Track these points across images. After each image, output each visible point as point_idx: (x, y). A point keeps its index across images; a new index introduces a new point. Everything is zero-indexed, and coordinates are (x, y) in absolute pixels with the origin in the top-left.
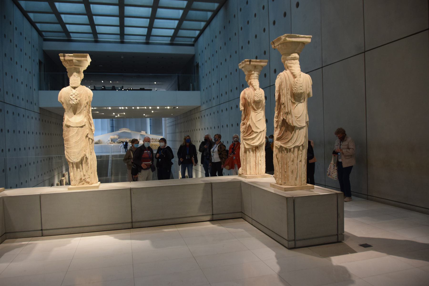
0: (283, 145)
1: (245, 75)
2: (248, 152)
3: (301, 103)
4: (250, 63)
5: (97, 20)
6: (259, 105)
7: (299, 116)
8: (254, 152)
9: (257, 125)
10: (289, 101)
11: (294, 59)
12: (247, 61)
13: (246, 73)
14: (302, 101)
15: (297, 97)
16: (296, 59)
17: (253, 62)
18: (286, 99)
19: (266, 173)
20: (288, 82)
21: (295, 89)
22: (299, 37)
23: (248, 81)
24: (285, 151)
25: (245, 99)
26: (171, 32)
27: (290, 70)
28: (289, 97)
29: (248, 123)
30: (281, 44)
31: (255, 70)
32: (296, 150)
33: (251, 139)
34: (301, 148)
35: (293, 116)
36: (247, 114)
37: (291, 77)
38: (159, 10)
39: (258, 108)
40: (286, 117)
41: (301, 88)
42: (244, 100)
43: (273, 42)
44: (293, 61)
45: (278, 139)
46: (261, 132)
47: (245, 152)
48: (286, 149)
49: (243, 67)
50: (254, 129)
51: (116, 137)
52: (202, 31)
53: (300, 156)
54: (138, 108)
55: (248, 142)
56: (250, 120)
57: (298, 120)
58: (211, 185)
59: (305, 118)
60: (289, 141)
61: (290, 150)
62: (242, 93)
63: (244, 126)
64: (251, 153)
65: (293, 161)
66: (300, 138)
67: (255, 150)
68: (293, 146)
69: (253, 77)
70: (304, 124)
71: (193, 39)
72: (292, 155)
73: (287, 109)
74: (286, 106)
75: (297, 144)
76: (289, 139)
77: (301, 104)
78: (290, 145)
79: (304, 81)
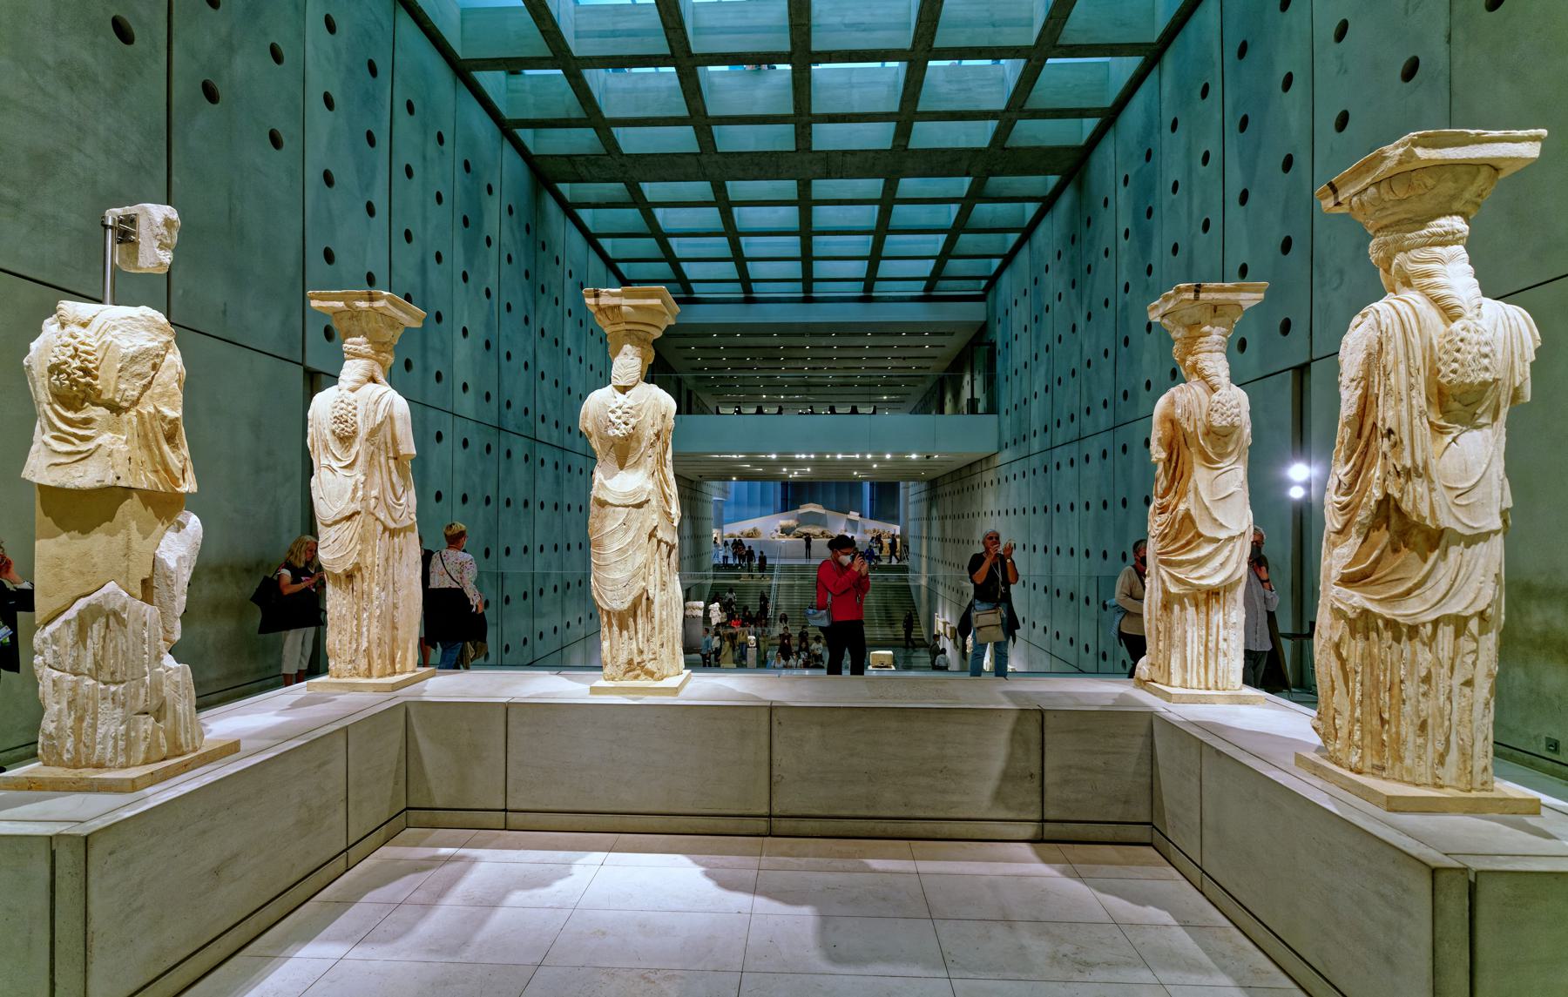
0: (1375, 608)
1: (1172, 342)
2: (1176, 608)
4: (1197, 298)
5: (750, 246)
6: (1226, 444)
7: (1468, 484)
8: (1203, 609)
9: (1216, 515)
10: (1416, 422)
11: (1444, 240)
12: (1187, 290)
13: (1178, 333)
14: (1482, 420)
15: (1456, 403)
16: (1456, 242)
17: (1209, 290)
18: (1404, 414)
19: (1246, 681)
20: (1416, 341)
22: (1479, 140)
23: (1184, 361)
24: (1388, 635)
25: (1173, 422)
26: (926, 268)
27: (1423, 290)
28: (1420, 401)
29: (1182, 507)
30: (1377, 184)
31: (1215, 321)
32: (1447, 632)
33: (1191, 562)
34: (1474, 625)
35: (1438, 486)
36: (1177, 472)
37: (1432, 315)
38: (897, 209)
39: (1222, 456)
40: (1402, 490)
41: (1486, 361)
42: (1168, 425)
43: (1331, 186)
44: (1438, 249)
45: (1348, 581)
46: (1231, 539)
47: (1167, 606)
48: (1391, 624)
49: (1163, 316)
50: (1206, 529)
51: (792, 523)
52: (1008, 259)
53: (1469, 659)
54: (839, 456)
55: (1179, 573)
56: (1191, 495)
57: (1458, 501)
58: (1039, 717)
59: (1497, 494)
60: (1408, 593)
61: (1413, 631)
62: (1162, 401)
63: (1164, 517)
64: (1191, 611)
65: (1427, 679)
66: (1473, 580)
67: (1207, 603)
68: (1433, 616)
69: (1205, 347)
70: (1497, 524)
71: (984, 283)
72: (1425, 656)
73: (1407, 453)
74: (1406, 442)
75: (1454, 607)
76: (1410, 584)
78: (1411, 610)
79: (1501, 333)
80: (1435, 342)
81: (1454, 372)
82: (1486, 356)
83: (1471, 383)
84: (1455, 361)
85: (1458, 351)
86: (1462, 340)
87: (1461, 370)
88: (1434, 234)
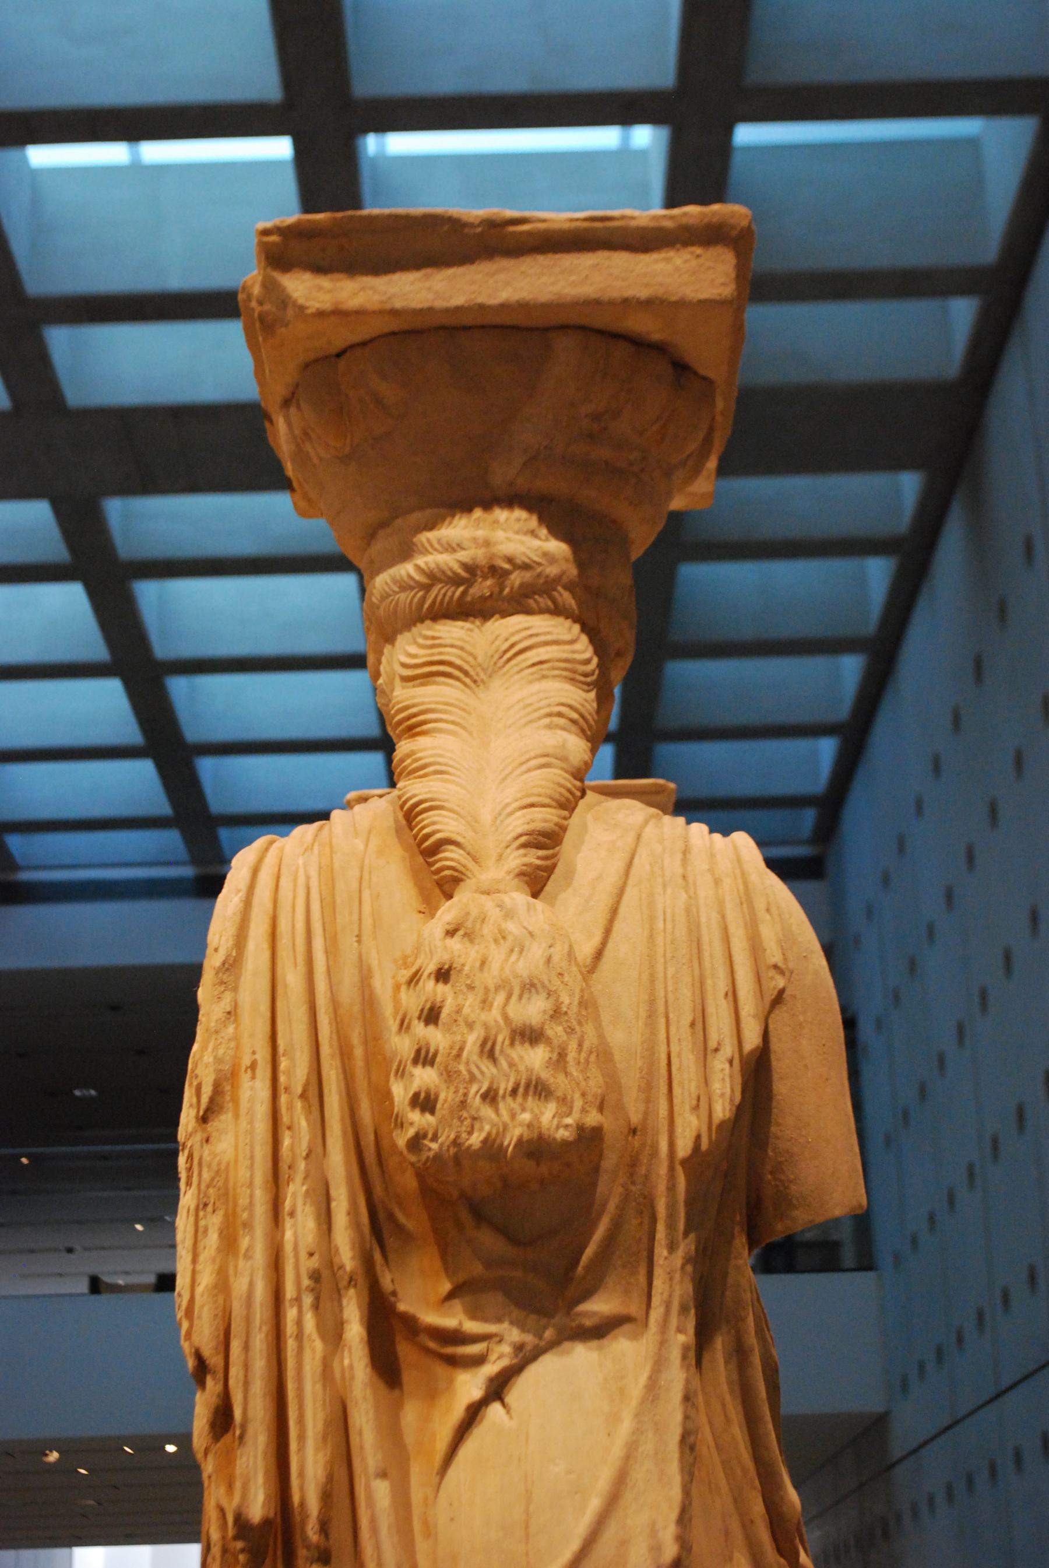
3: (600, 1331)
10: (302, 1318)
11: (479, 595)
21: (424, 1077)
37: (393, 878)
41: (535, 1059)
44: (452, 631)
73: (253, 1458)
74: (253, 1408)
77: (582, 1357)
80: (382, 986)
81: (425, 1102)
82: (531, 1036)
83: (491, 1149)
84: (424, 1057)
85: (432, 1016)
86: (443, 975)
87: (446, 1097)
88: (434, 577)
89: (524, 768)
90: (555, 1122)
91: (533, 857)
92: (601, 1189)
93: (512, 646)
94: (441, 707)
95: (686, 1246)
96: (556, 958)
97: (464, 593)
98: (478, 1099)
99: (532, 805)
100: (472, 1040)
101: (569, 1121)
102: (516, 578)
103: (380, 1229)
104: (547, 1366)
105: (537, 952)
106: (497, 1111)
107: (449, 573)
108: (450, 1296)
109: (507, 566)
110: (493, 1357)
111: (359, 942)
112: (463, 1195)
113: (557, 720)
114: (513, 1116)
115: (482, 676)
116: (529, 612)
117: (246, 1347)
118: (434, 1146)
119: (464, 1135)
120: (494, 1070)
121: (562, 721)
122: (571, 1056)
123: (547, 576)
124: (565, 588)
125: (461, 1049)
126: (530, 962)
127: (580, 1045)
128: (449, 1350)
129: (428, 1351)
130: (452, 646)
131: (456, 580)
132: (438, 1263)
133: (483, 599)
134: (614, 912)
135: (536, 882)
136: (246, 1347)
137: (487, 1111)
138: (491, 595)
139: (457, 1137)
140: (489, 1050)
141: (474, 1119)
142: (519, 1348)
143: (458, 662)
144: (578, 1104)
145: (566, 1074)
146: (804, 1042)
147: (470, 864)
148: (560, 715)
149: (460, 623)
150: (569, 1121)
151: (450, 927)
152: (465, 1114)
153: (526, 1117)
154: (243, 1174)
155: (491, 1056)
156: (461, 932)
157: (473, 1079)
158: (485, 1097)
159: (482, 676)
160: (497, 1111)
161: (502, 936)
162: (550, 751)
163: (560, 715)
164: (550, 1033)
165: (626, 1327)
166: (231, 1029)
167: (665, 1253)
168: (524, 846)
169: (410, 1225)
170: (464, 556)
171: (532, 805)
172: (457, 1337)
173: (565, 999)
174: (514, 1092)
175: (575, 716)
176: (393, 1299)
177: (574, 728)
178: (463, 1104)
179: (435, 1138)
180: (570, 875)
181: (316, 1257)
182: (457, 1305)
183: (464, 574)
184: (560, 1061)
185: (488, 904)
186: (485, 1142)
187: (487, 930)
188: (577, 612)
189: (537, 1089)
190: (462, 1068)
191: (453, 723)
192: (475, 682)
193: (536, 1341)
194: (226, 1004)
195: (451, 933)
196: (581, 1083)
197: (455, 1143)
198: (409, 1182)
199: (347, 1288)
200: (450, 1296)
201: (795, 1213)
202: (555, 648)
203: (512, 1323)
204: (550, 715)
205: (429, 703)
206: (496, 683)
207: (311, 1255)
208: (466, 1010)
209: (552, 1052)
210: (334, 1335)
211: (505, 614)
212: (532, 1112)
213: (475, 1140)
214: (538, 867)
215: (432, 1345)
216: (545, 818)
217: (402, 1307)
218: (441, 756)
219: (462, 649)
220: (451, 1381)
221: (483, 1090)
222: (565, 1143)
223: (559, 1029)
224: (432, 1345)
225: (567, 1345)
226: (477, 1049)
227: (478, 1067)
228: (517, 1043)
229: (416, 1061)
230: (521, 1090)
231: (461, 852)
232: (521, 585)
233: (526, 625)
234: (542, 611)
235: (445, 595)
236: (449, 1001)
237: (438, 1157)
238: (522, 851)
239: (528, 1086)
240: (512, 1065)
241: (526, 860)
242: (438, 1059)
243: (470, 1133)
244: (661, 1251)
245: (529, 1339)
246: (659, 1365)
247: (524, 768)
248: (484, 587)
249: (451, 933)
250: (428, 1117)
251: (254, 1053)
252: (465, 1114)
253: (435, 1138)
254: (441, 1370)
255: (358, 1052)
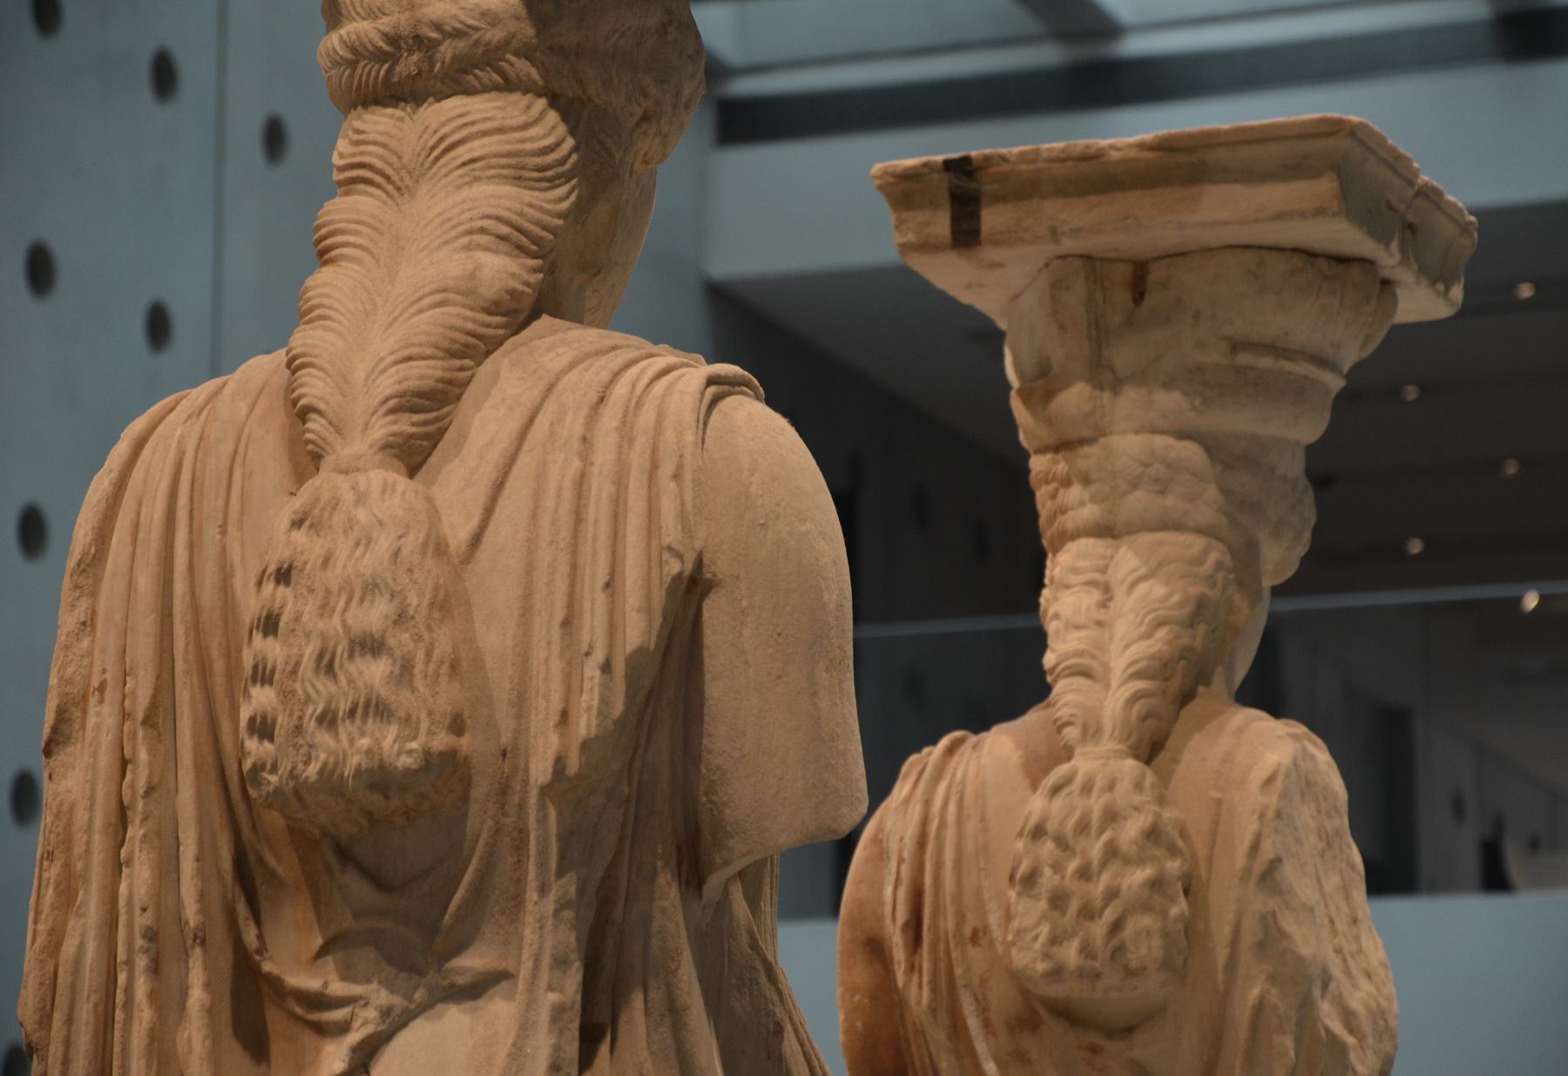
3: (474, 990)
14: (472, 961)
21: (262, 698)
37: (268, 451)
41: (376, 671)
77: (454, 1018)
81: (263, 728)
82: (370, 645)
83: (330, 780)
84: (262, 675)
86: (284, 575)
87: (283, 723)
89: (416, 307)
90: (396, 748)
91: (406, 424)
92: (472, 822)
93: (441, 140)
94: (351, 226)
95: (568, 885)
96: (405, 552)
97: (389, 72)
98: (313, 723)
99: (410, 359)
100: (310, 651)
101: (414, 745)
102: (447, 50)
103: (248, 879)
104: (417, 1033)
105: (384, 545)
106: (336, 736)
107: (370, 47)
108: (323, 952)
109: (434, 35)
110: (356, 1024)
111: (224, 533)
112: (325, 833)
113: (478, 238)
114: (351, 741)
115: (408, 181)
116: (468, 91)
117: (69, 1020)
118: (274, 779)
119: (300, 766)
120: (333, 688)
121: (484, 239)
122: (419, 667)
123: (488, 44)
124: (517, 54)
125: (298, 664)
126: (373, 560)
127: (429, 655)
128: (315, 1016)
129: (298, 1018)
130: (375, 143)
131: (379, 56)
132: (311, 914)
133: (413, 78)
134: (499, 486)
135: (413, 455)
136: (69, 1020)
137: (324, 738)
138: (419, 73)
139: (293, 768)
140: (327, 665)
141: (311, 746)
142: (386, 1012)
143: (379, 164)
144: (424, 725)
145: (413, 690)
146: (747, 633)
147: (331, 436)
148: (482, 231)
149: (390, 111)
150: (414, 745)
151: (296, 517)
152: (301, 741)
153: (365, 742)
154: (81, 817)
155: (330, 670)
156: (307, 523)
157: (308, 700)
158: (320, 720)
159: (408, 181)
160: (336, 736)
161: (351, 523)
162: (451, 283)
163: (482, 231)
164: (392, 642)
165: (504, 984)
166: (85, 643)
167: (535, 897)
168: (392, 411)
169: (280, 870)
170: (385, 23)
171: (410, 359)
172: (319, 1001)
173: (413, 600)
174: (352, 713)
175: (505, 230)
176: (257, 958)
177: (504, 246)
178: (298, 730)
179: (274, 770)
180: (459, 444)
181: (150, 912)
182: (329, 963)
183: (386, 48)
184: (405, 671)
185: (343, 484)
186: (321, 772)
187: (338, 519)
188: (541, 83)
189: (374, 708)
190: (298, 686)
191: (360, 247)
192: (398, 189)
193: (406, 1004)
194: (80, 613)
195: (297, 524)
196: (429, 700)
197: (293, 775)
198: (274, 820)
199: (193, 947)
200: (323, 952)
201: (731, 842)
202: (496, 138)
203: (380, 983)
204: (470, 232)
205: (340, 221)
206: (423, 189)
207: (144, 910)
208: (305, 618)
209: (394, 664)
210: (169, 1004)
211: (441, 96)
212: (372, 735)
213: (312, 771)
214: (412, 436)
215: (299, 1010)
216: (426, 372)
217: (267, 967)
218: (327, 296)
219: (385, 146)
220: (318, 1051)
221: (319, 711)
222: (408, 773)
223: (405, 637)
224: (299, 1010)
225: (440, 1007)
226: (312, 664)
227: (313, 685)
228: (357, 655)
229: (254, 680)
230: (360, 711)
231: (323, 421)
232: (454, 58)
233: (462, 110)
234: (486, 89)
235: (369, 74)
236: (289, 607)
237: (278, 791)
238: (391, 418)
239: (367, 705)
240: (350, 681)
241: (395, 428)
242: (277, 676)
243: (307, 763)
244: (532, 895)
245: (397, 1001)
246: (525, 1028)
247: (416, 307)
248: (409, 64)
249: (297, 524)
250: (267, 744)
251: (104, 671)
252: (301, 741)
253: (274, 770)
254: (308, 1038)
255: (219, 667)
